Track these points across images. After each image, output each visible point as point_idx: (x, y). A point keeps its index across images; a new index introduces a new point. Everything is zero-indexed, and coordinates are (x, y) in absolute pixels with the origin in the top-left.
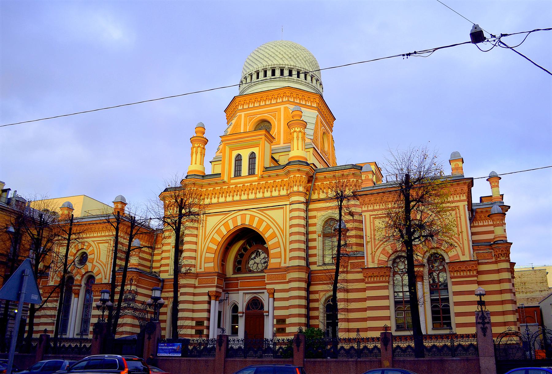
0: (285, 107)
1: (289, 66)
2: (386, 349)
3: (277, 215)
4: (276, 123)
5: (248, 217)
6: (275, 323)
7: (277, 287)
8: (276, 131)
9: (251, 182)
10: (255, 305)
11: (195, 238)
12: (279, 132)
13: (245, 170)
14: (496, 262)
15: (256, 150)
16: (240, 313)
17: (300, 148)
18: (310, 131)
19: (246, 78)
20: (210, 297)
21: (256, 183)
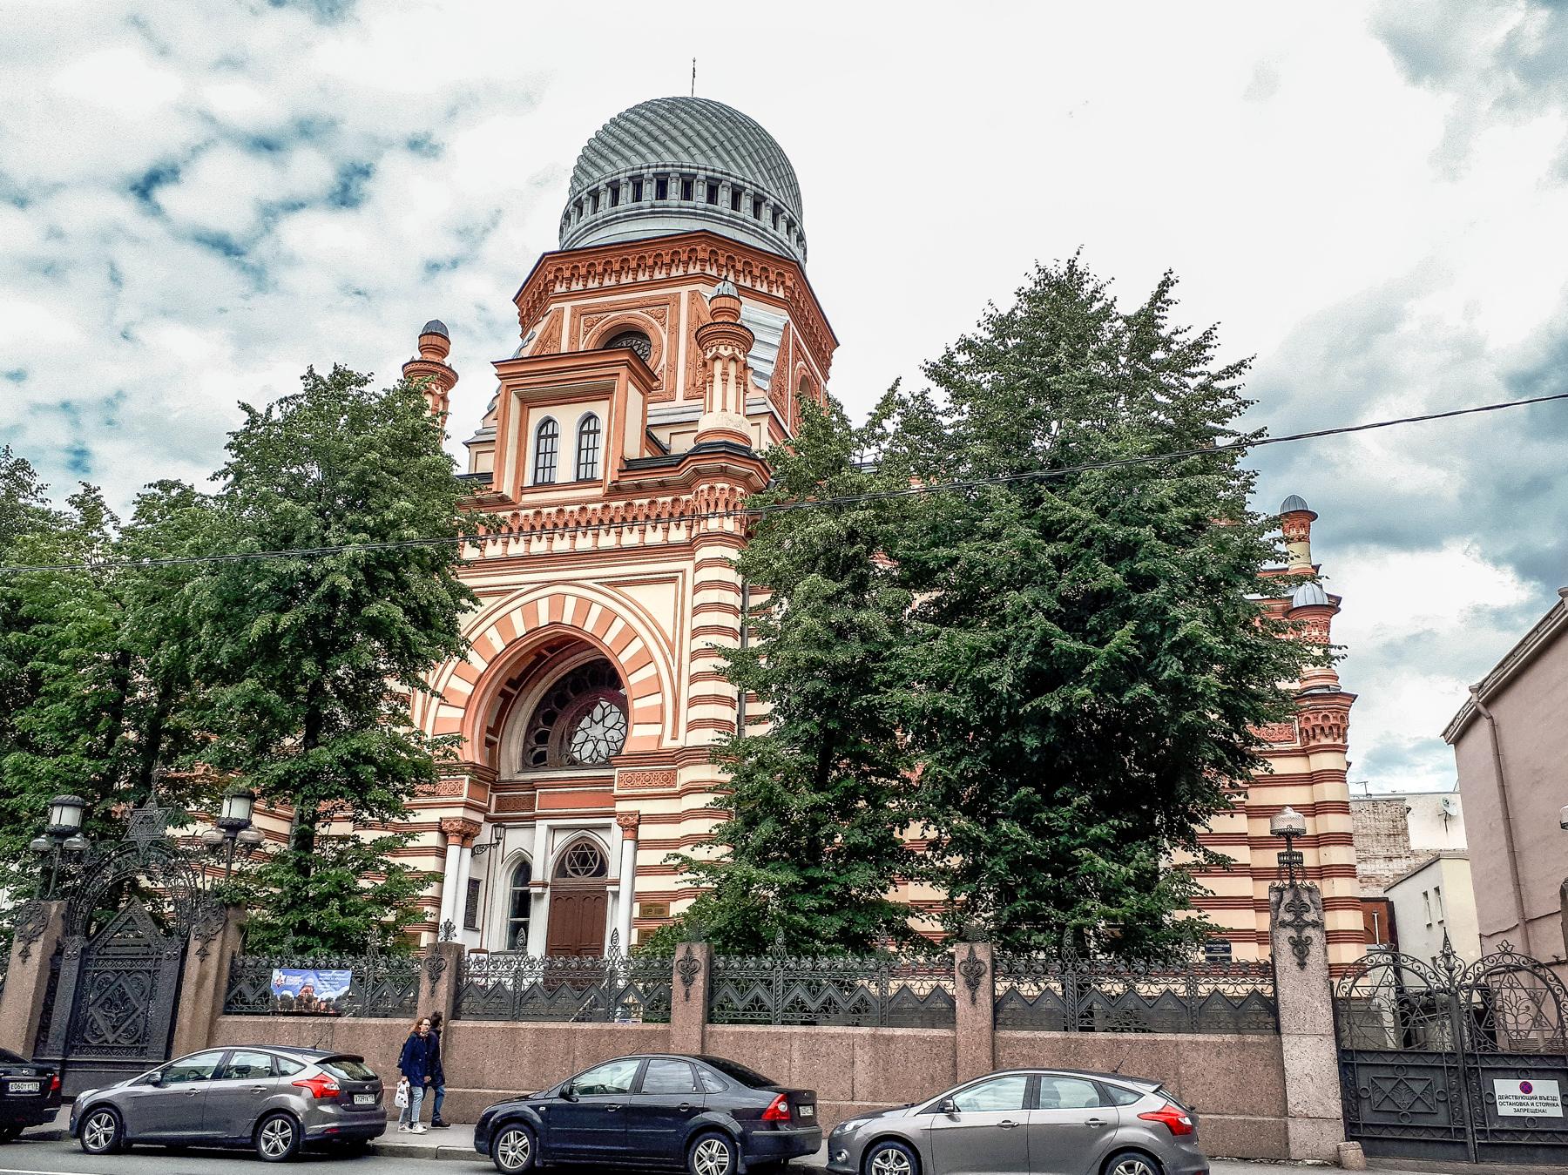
0: (692, 293)
1: (710, 174)
2: (974, 1000)
3: (657, 601)
4: (665, 338)
5: (570, 603)
6: (636, 914)
7: (646, 808)
8: (664, 361)
9: (583, 505)
10: (584, 859)
12: (673, 367)
13: (565, 470)
14: (1305, 753)
16: (536, 885)
17: (731, 405)
18: (763, 357)
19: (579, 205)
20: (444, 835)
21: (599, 506)
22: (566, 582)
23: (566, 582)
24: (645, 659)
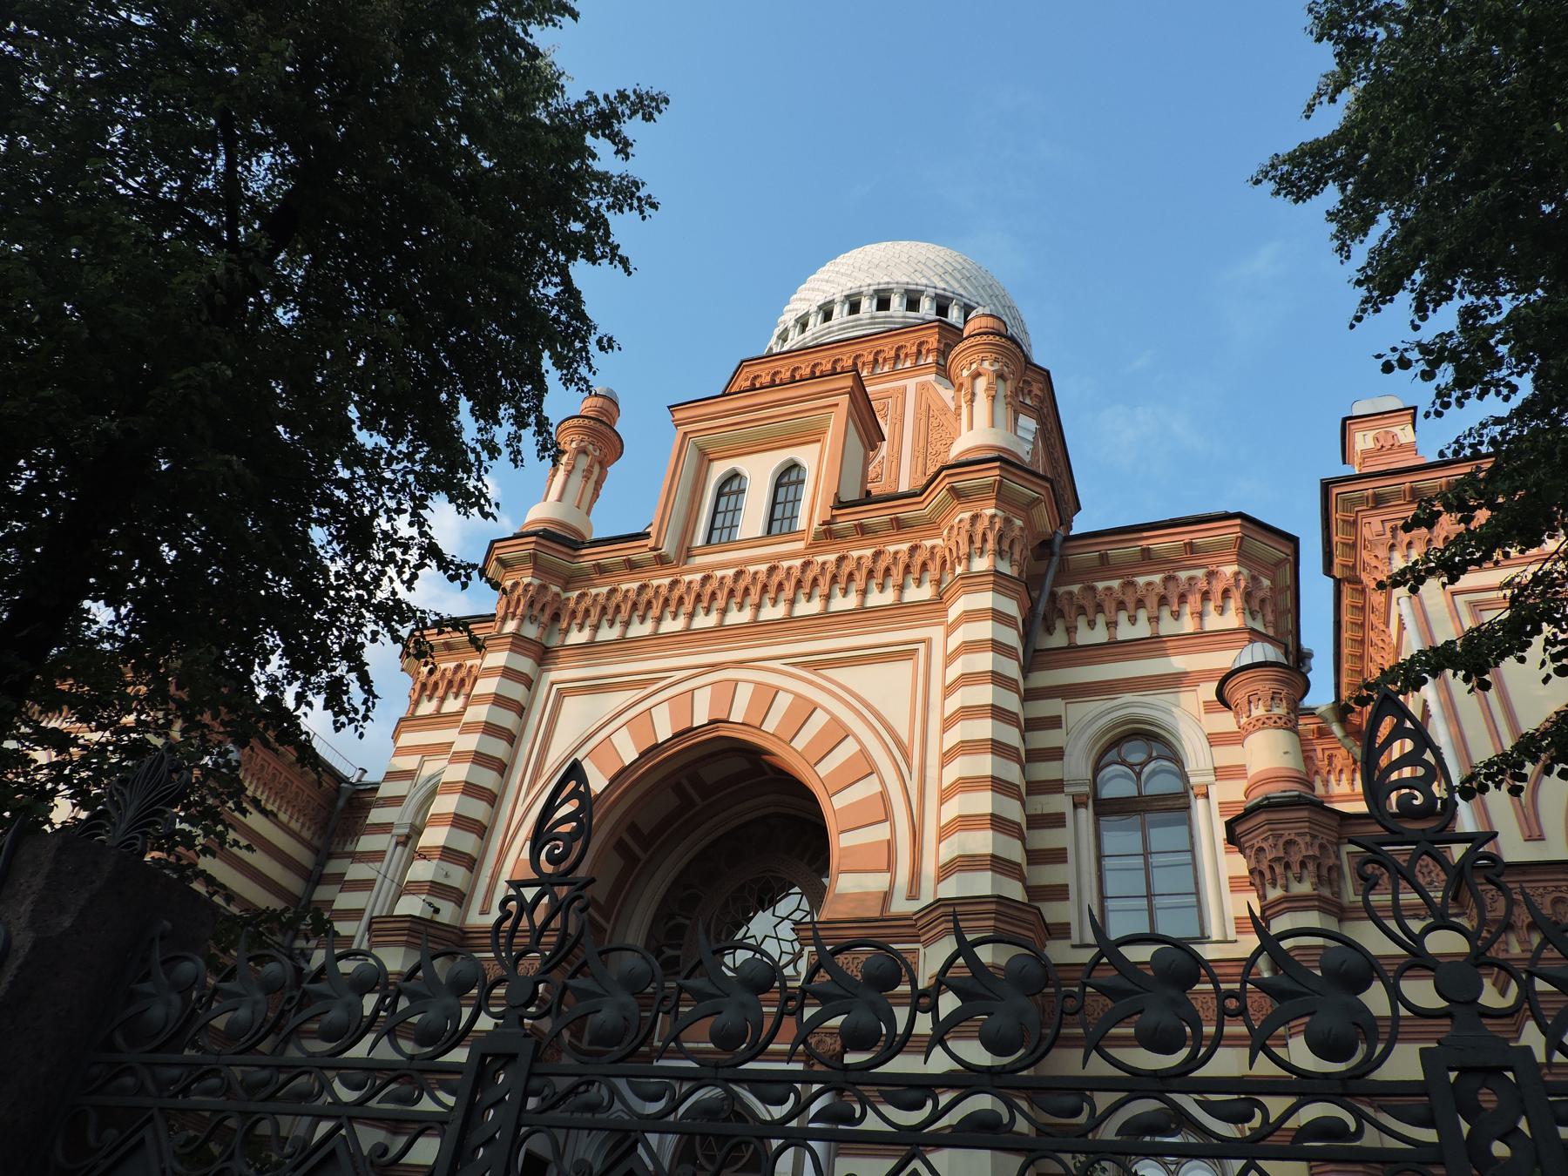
3: (886, 686)
5: (744, 694)
11: (494, 774)
15: (806, 456)
22: (740, 664)
23: (740, 664)
24: (864, 767)
